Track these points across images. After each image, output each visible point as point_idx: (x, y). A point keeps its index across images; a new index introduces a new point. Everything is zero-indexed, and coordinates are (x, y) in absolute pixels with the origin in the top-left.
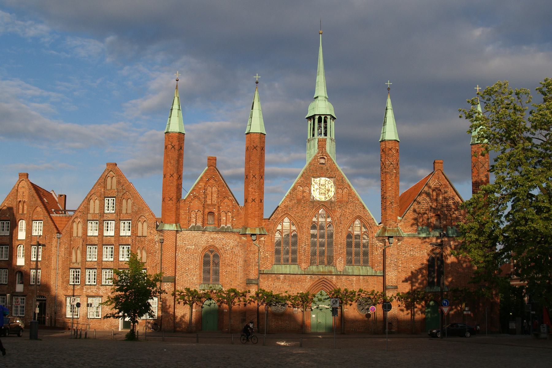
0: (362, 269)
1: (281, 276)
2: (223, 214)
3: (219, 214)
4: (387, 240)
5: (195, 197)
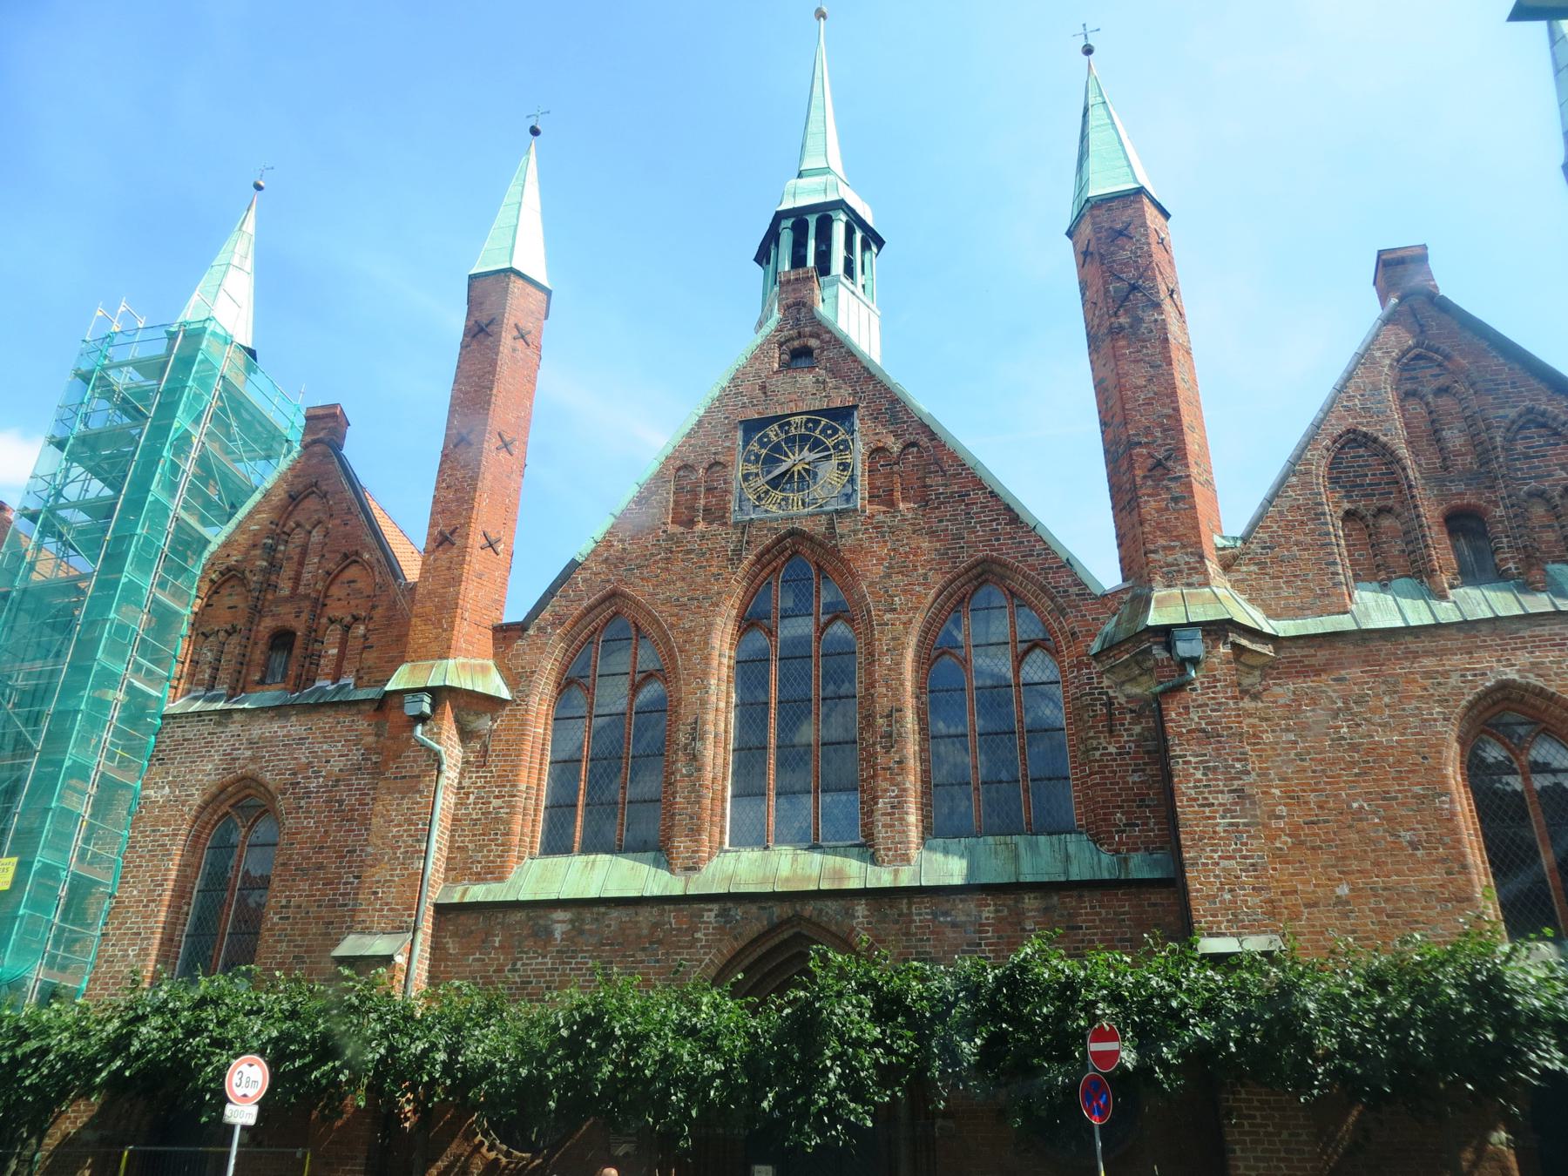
0: (1033, 848)
1: (560, 915)
2: (333, 636)
3: (314, 636)
4: (1159, 653)
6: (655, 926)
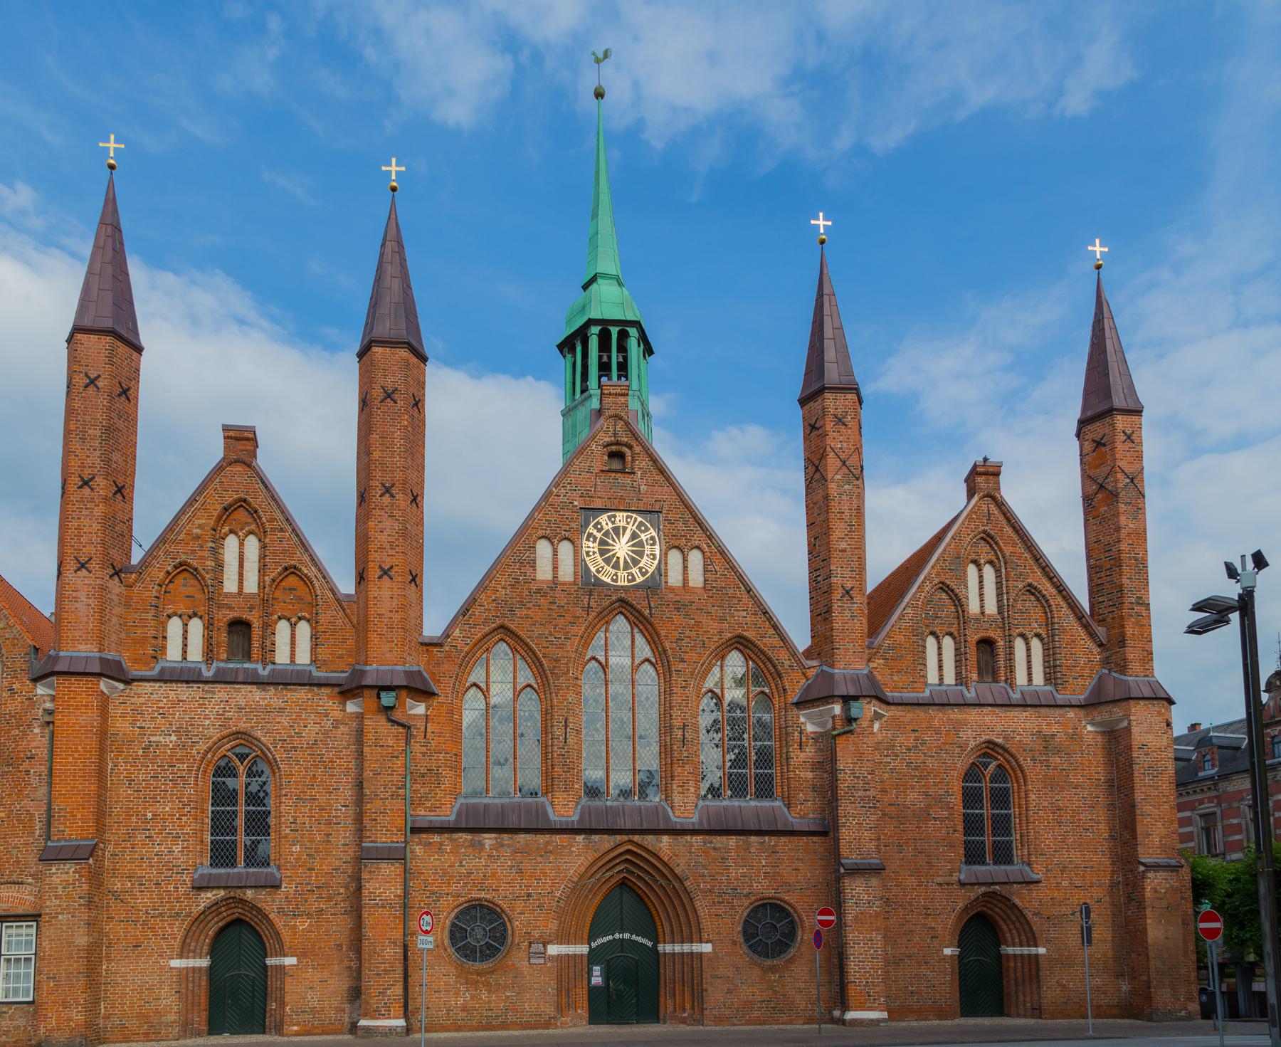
5: (183, 567)
6: (547, 843)
